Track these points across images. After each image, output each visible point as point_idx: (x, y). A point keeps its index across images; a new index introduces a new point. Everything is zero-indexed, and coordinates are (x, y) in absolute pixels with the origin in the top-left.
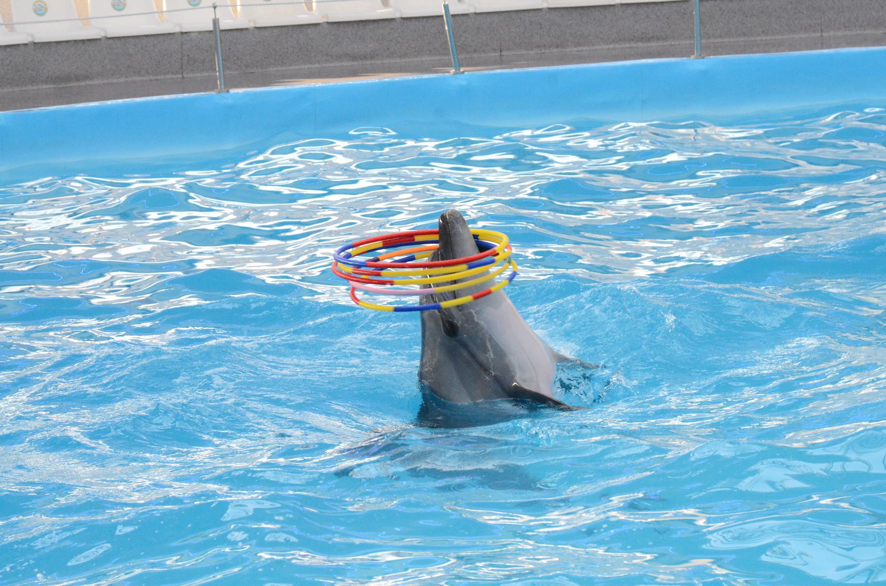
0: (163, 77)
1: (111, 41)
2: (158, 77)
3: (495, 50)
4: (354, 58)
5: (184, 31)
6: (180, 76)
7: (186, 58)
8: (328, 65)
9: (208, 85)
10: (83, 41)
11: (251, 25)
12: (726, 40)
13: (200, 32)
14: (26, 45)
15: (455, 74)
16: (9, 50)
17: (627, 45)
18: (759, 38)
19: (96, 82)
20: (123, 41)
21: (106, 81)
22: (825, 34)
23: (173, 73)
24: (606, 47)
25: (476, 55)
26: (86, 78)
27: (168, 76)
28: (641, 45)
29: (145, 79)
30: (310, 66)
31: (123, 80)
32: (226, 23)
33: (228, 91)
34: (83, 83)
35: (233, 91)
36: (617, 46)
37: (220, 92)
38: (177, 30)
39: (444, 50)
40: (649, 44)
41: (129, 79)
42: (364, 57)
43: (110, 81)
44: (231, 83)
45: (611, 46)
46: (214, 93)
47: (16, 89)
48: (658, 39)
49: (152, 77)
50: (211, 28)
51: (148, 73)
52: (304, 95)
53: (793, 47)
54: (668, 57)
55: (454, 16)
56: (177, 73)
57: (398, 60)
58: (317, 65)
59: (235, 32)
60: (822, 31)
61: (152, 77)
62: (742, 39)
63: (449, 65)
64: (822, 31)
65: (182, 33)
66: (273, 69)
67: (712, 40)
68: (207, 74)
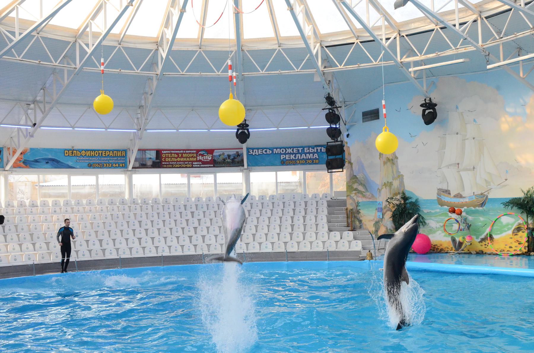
32: (36, 263)
39: (75, 267)
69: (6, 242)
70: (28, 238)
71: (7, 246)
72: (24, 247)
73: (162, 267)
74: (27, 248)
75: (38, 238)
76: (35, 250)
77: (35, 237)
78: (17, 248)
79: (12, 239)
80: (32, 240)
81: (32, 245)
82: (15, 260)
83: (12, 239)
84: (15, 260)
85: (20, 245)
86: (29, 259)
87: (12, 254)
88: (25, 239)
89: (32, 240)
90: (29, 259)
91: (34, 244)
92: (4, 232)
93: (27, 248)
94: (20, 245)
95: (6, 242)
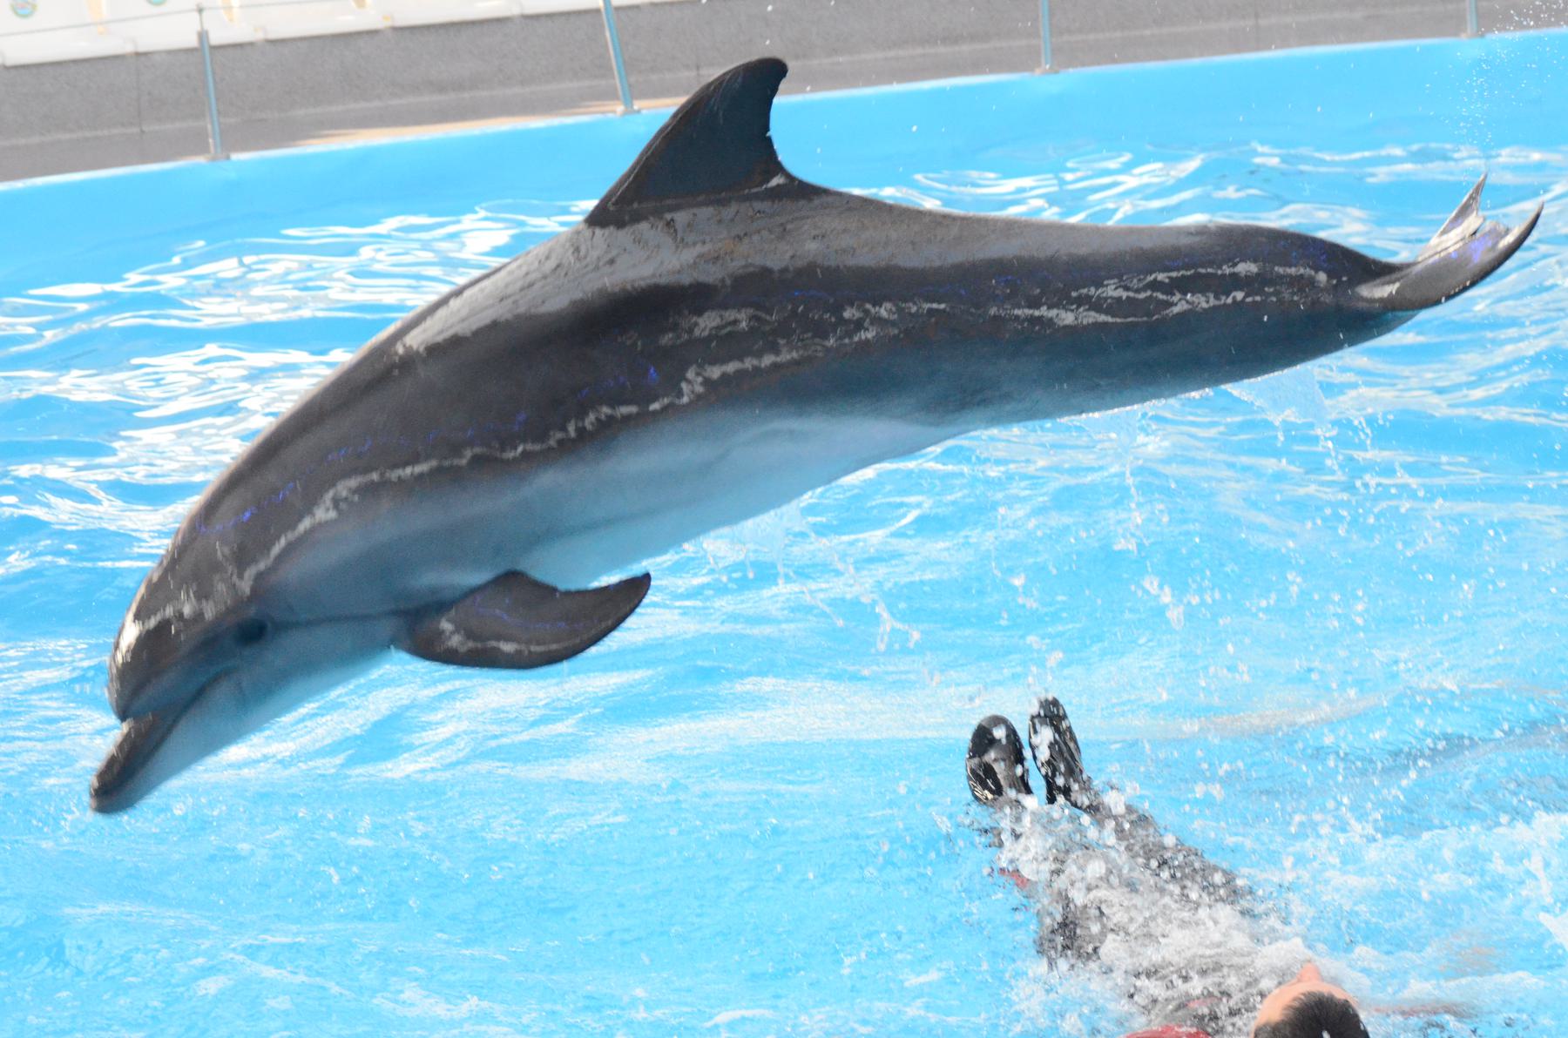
0: (106, 132)
2: (99, 133)
3: (687, 67)
4: (441, 88)
5: (142, 49)
6: (135, 130)
8: (395, 102)
9: (193, 144)
12: (1091, 37)
13: (169, 52)
15: (626, 113)
17: (919, 51)
18: (1148, 32)
22: (1263, 22)
23: (123, 125)
24: (880, 55)
25: (654, 77)
27: (115, 131)
28: (942, 49)
30: (363, 105)
31: (36, 139)
33: (228, 158)
35: (235, 157)
36: (901, 53)
37: (214, 159)
38: (129, 48)
39: (604, 70)
40: (957, 48)
42: (459, 86)
44: (236, 139)
45: (892, 54)
46: (200, 160)
48: (973, 38)
49: (88, 134)
50: (193, 42)
52: (365, 158)
53: (1208, 45)
54: (992, 72)
55: (618, 9)
57: (517, 90)
58: (377, 103)
60: (1257, 16)
61: (88, 134)
62: (1118, 34)
63: (609, 95)
64: (1257, 16)
65: (138, 54)
66: (300, 113)
67: (1066, 38)
73: (1466, 48)
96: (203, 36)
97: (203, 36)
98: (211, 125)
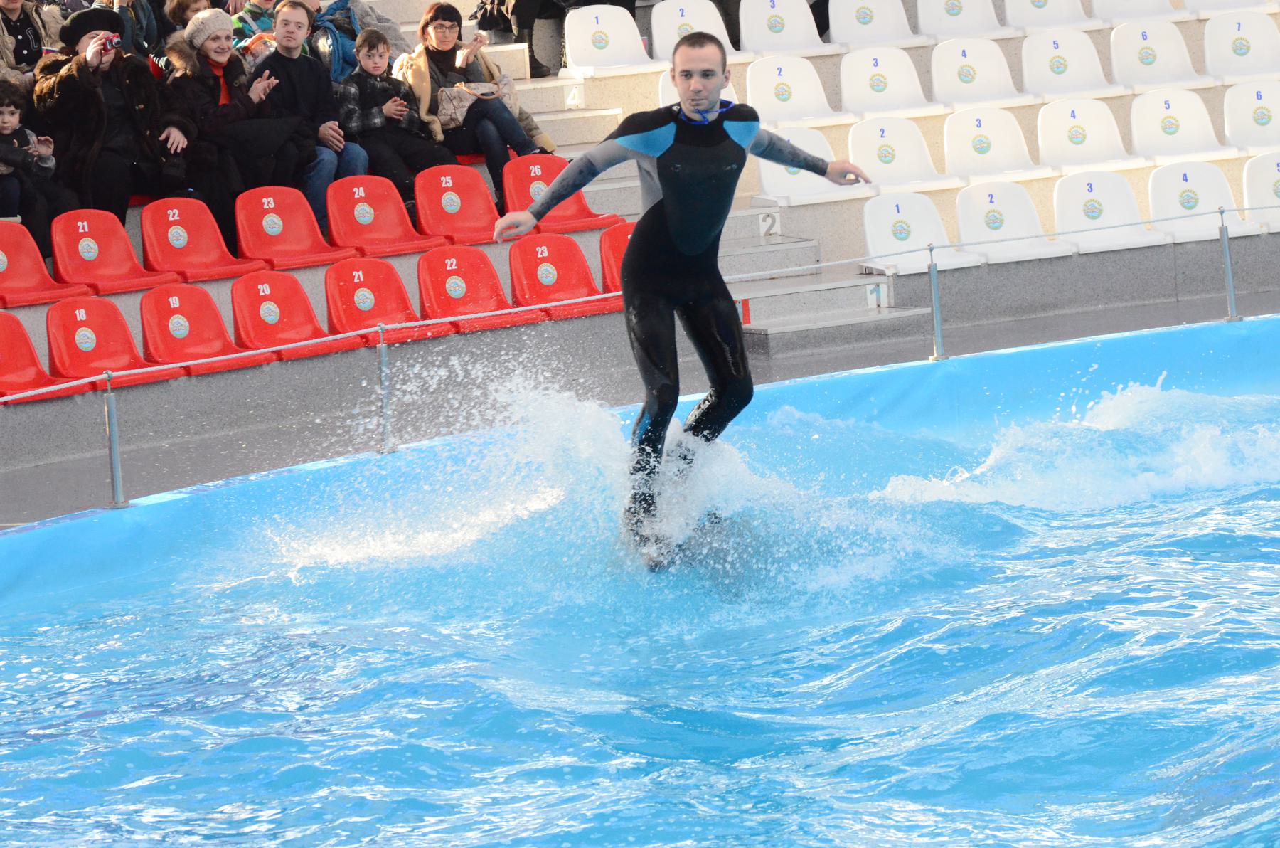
1: (1085, 258)
6: (1174, 300)
7: (1181, 276)
10: (1050, 259)
11: (1264, 230)
14: (978, 267)
16: (957, 275)
19: (1067, 311)
20: (1100, 257)
21: (1080, 310)
26: (1055, 306)
27: (1158, 301)
29: (1129, 304)
34: (1051, 314)
38: (1169, 240)
41: (1110, 306)
43: (1085, 309)
47: (968, 325)
49: (1140, 303)
51: (1133, 298)
56: (1170, 296)
59: (1243, 242)
61: (1140, 303)
68: (1209, 296)
69: (1020, 87)
70: (1172, 49)
71: (1027, 117)
72: (1145, 118)
74: (1170, 128)
75: (1241, 49)
76: (1222, 140)
77: (1217, 43)
78: (1100, 125)
79: (1058, 67)
80: (1199, 66)
81: (1196, 100)
82: (1093, 211)
83: (1058, 67)
84: (1093, 211)
85: (1121, 107)
86: (1189, 202)
87: (1069, 171)
88: (1147, 58)
89: (1199, 66)
90: (1189, 202)
91: (1213, 98)
92: (1002, 20)
93: (1170, 128)
94: (1121, 107)
95: (1020, 87)
96: (1223, 230)
97: (1223, 230)
98: (1230, 295)
